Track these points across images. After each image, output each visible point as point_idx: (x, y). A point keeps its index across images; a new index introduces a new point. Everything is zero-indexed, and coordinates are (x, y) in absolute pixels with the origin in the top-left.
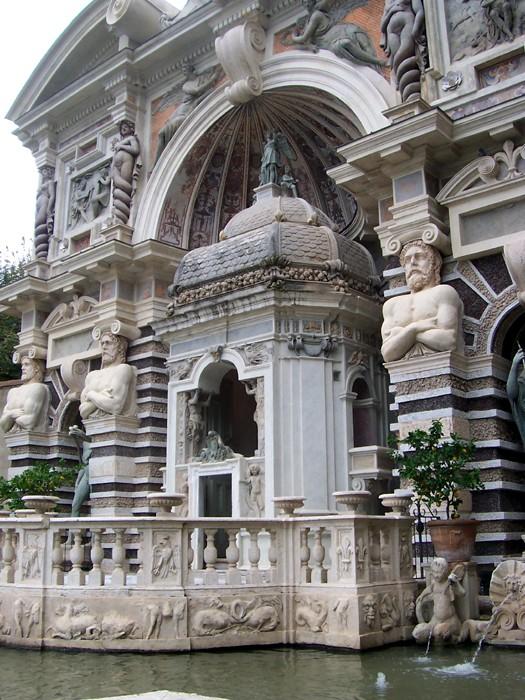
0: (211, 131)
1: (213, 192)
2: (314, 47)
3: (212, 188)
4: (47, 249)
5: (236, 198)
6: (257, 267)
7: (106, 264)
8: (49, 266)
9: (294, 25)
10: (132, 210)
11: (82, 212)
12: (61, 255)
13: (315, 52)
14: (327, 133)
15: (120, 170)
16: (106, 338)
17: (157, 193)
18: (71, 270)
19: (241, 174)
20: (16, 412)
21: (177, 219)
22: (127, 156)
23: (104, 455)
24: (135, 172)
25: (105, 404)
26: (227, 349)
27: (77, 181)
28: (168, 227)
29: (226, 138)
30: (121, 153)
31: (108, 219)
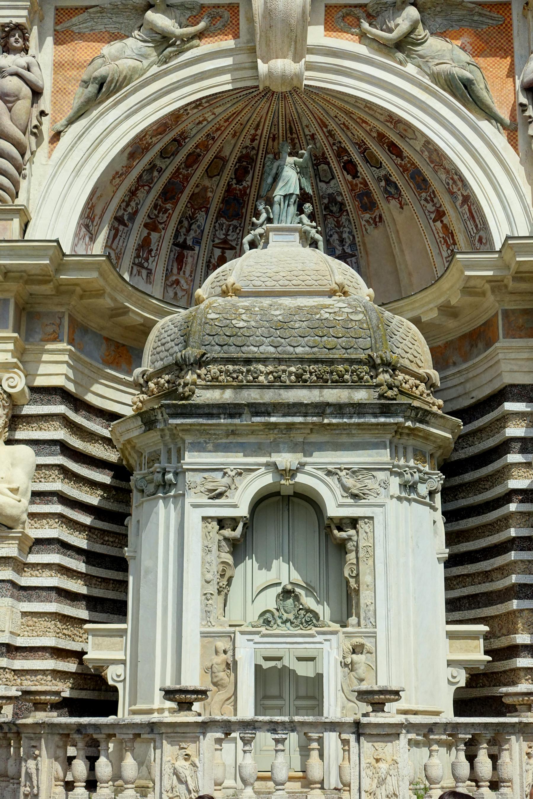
0: (189, 108)
1: (141, 194)
2: (400, 56)
3: (143, 186)
5: (166, 210)
6: (360, 362)
9: (366, 5)
10: (23, 184)
13: (401, 63)
14: (350, 167)
15: (10, 110)
17: (77, 171)
19: (187, 178)
21: (93, 222)
22: (26, 91)
24: (35, 122)
25: (10, 511)
26: (307, 468)
28: (84, 229)
29: (200, 123)
30: (15, 79)
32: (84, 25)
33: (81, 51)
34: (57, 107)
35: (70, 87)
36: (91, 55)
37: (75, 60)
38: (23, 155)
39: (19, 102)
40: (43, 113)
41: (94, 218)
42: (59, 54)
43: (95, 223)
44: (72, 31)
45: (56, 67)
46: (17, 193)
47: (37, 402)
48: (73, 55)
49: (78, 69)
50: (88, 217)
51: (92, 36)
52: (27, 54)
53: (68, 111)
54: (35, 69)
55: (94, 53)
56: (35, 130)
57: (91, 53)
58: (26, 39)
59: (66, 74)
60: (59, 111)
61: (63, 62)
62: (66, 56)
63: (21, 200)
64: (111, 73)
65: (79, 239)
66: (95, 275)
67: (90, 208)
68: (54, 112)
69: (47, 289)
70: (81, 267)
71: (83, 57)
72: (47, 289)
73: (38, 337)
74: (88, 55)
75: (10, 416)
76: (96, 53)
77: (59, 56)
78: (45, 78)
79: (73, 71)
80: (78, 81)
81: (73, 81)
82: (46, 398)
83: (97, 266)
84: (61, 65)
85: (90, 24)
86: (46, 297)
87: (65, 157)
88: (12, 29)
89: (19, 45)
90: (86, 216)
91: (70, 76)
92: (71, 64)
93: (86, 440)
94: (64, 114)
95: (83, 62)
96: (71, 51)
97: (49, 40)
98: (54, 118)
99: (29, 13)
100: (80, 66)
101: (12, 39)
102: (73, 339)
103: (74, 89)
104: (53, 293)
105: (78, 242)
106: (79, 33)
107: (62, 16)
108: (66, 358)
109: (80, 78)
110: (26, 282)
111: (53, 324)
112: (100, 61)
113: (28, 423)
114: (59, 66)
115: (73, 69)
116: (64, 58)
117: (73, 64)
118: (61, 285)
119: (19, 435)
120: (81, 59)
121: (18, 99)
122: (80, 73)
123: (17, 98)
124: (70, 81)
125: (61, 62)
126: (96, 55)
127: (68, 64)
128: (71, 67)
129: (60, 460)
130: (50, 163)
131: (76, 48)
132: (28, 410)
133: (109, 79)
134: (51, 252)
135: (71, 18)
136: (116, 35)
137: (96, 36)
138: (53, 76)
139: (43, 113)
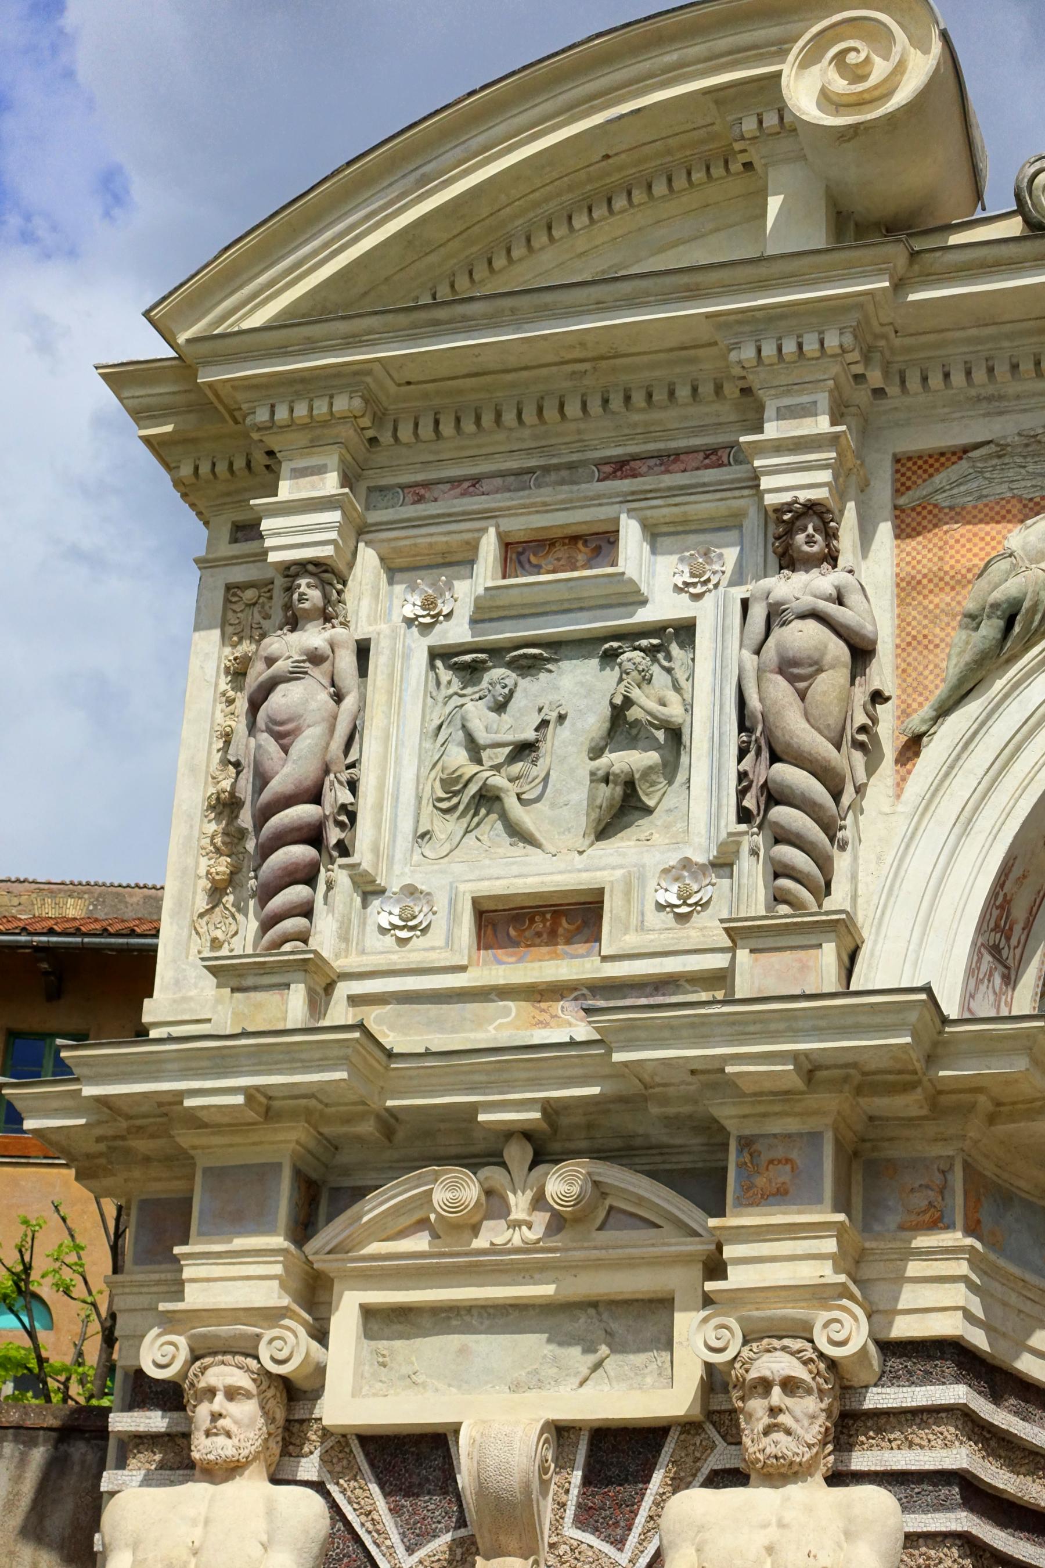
4: (307, 911)
7: (811, 1069)
8: (329, 988)
10: (842, 862)
11: (511, 802)
12: (380, 951)
15: (802, 695)
16: (778, 1364)
17: (965, 821)
18: (617, 1057)
21: (1008, 939)
22: (838, 649)
24: (861, 718)
27: (463, 664)
28: (987, 958)
30: (811, 626)
31: (686, 864)
32: (962, 488)
33: (958, 546)
34: (909, 680)
35: (937, 630)
36: (982, 554)
37: (947, 568)
38: (837, 796)
39: (823, 675)
40: (878, 697)
41: (1011, 929)
42: (909, 559)
43: (1014, 941)
44: (936, 506)
45: (903, 589)
46: (828, 884)
47: (898, 1378)
48: (941, 559)
49: (953, 588)
50: (996, 928)
51: (981, 511)
52: (835, 566)
53: (937, 687)
54: (854, 598)
55: (988, 549)
56: (862, 737)
57: (982, 549)
58: (830, 535)
59: (926, 602)
60: (915, 690)
61: (919, 577)
62: (925, 561)
63: (838, 900)
64: (1030, 590)
65: (979, 982)
66: (1020, 1064)
67: (1001, 907)
68: (904, 691)
69: (908, 1104)
70: (987, 1046)
71: (963, 561)
72: (908, 1104)
73: (892, 1220)
74: (975, 555)
75: (836, 1413)
76: (993, 548)
77: (908, 563)
78: (879, 615)
79: (942, 595)
80: (954, 616)
81: (943, 616)
82: (919, 1367)
83: (1026, 1043)
84: (914, 583)
85: (974, 485)
86: (910, 1122)
87: (935, 791)
88: (798, 516)
89: (816, 549)
90: (992, 925)
91: (937, 606)
92: (936, 580)
93: (1023, 1470)
94: (926, 693)
95: (964, 571)
96: (935, 550)
97: (885, 530)
98: (903, 706)
99: (836, 477)
100: (959, 582)
101: (801, 538)
102: (979, 1222)
103: (948, 635)
104: (924, 1112)
105: (977, 988)
106: (951, 508)
107: (909, 474)
108: (962, 1268)
109: (958, 609)
110: (859, 1091)
111: (928, 1187)
112: (1004, 565)
113: (879, 1431)
114: (908, 587)
115: (942, 589)
116: (919, 567)
117: (941, 579)
118: (940, 1093)
119: (861, 1460)
120: (958, 567)
121: (821, 670)
122: (959, 598)
123: (818, 667)
124: (936, 617)
125: (913, 578)
126: (994, 554)
127: (930, 581)
128: (936, 585)
129: (960, 1520)
130: (900, 808)
131: (946, 543)
133: (1026, 605)
134: (913, 1017)
135: (931, 476)
136: (1037, 504)
137: (992, 509)
138: (897, 611)
139: (878, 697)
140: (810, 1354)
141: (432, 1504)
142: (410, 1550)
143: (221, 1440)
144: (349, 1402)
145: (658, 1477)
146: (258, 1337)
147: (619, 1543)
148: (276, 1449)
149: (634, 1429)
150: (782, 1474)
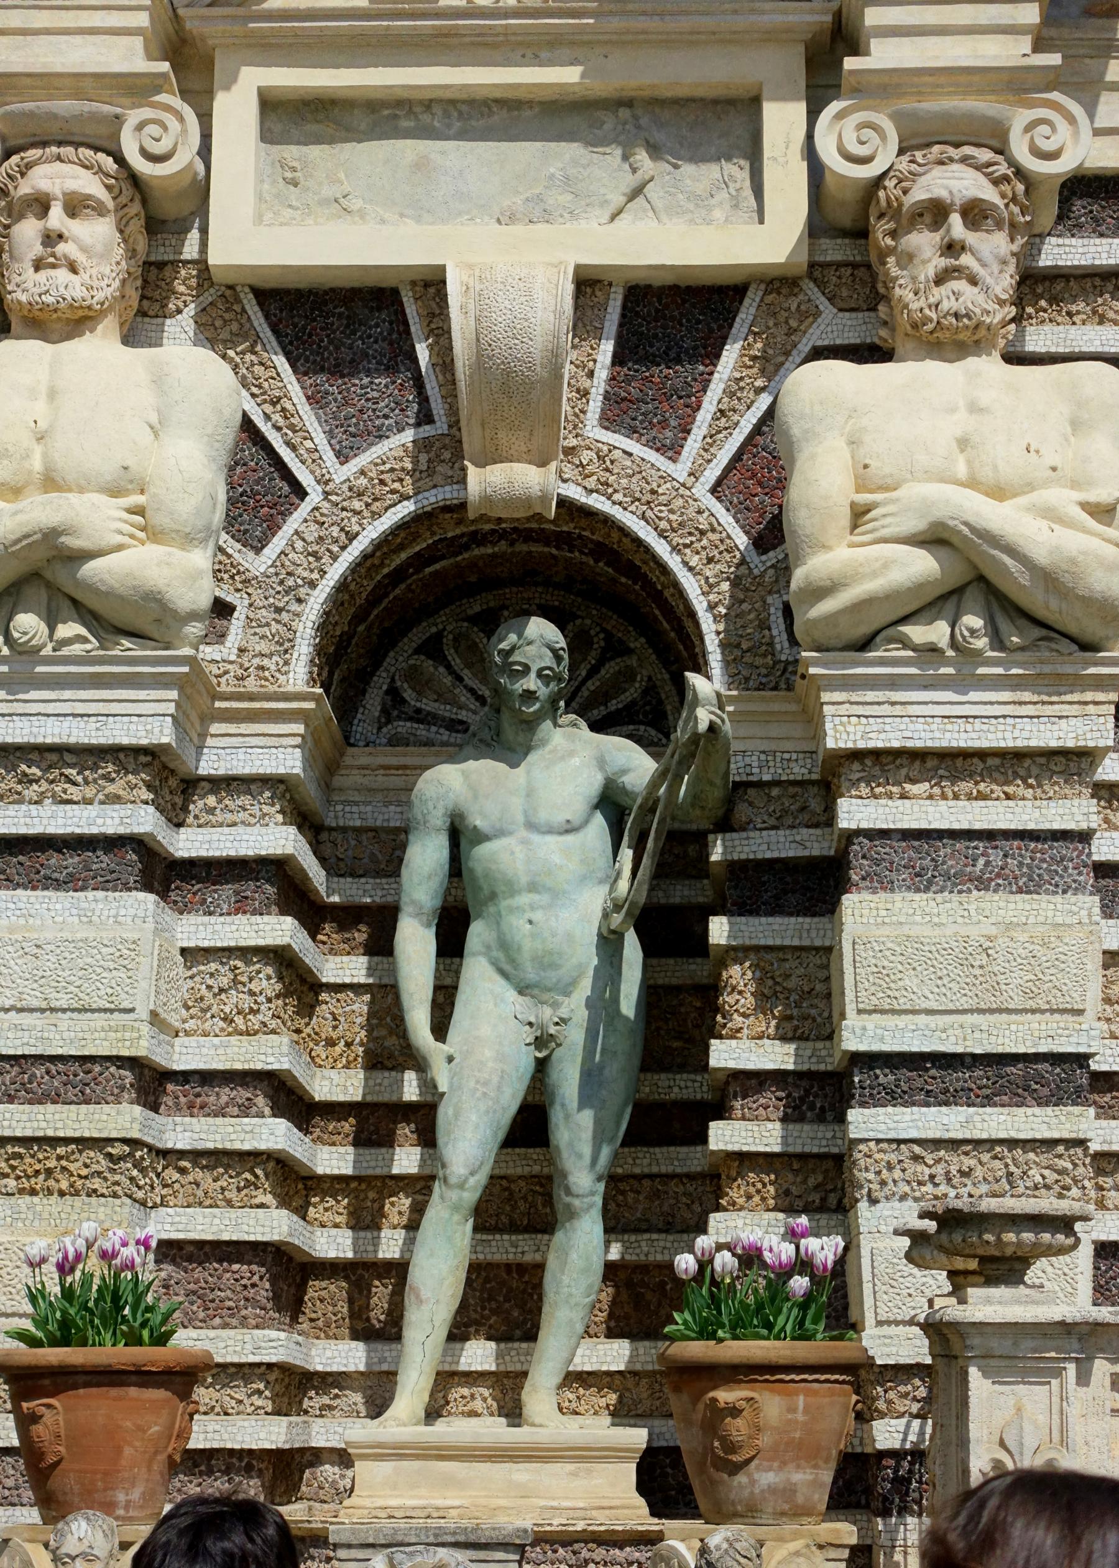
16: (957, 181)
20: (93, 517)
23: (982, 883)
47: (1080, 226)
113: (1054, 300)
119: (1038, 339)
132: (1065, 252)
140: (1003, 169)
141: (378, 388)
142: (343, 457)
143: (62, 275)
144: (257, 226)
145: (731, 354)
146: (119, 120)
147: (672, 451)
148: (134, 297)
149: (688, 288)
150: (953, 341)
